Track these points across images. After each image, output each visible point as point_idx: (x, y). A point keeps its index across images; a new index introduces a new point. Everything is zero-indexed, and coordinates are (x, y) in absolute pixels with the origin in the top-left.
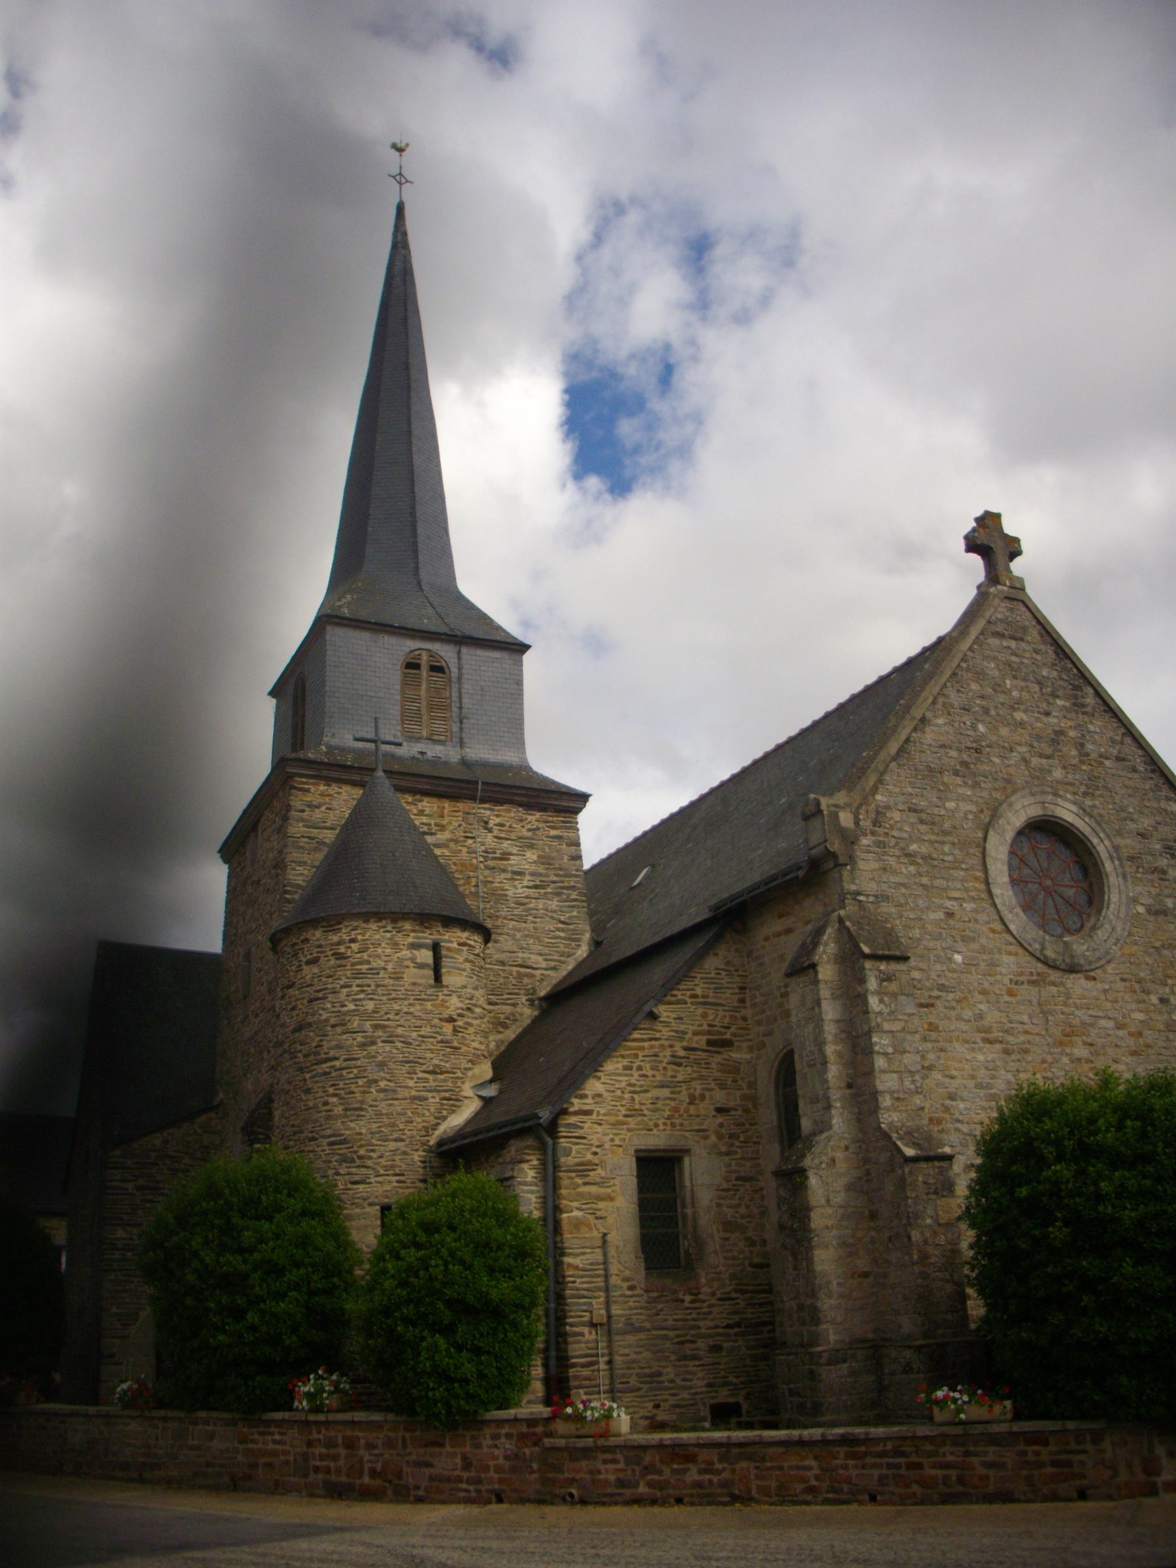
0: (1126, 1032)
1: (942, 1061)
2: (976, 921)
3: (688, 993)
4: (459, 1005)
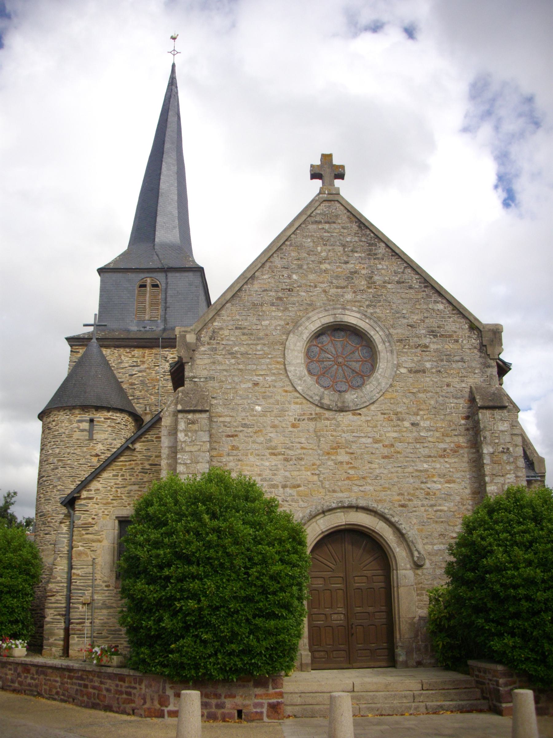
0: (381, 445)
1: (239, 467)
2: (275, 387)
3: (155, 436)
4: (102, 448)
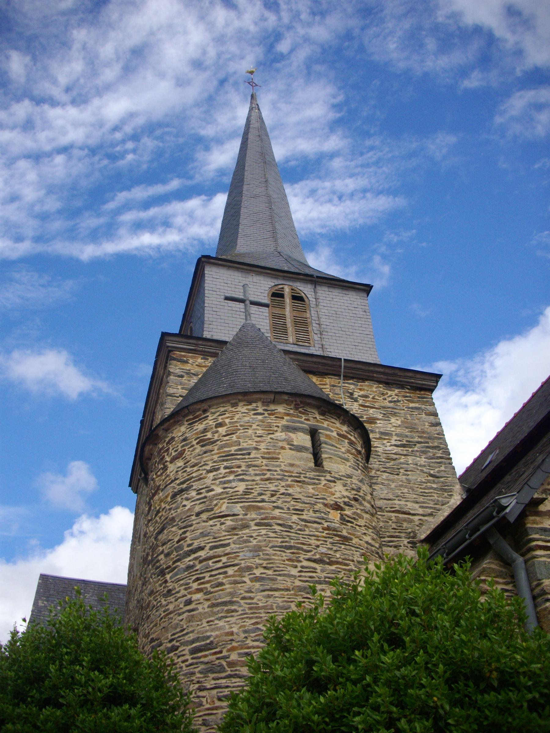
4: (346, 493)
